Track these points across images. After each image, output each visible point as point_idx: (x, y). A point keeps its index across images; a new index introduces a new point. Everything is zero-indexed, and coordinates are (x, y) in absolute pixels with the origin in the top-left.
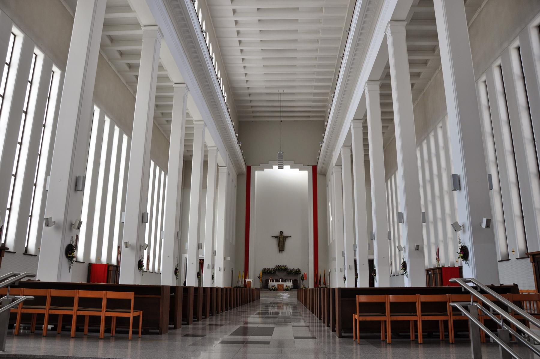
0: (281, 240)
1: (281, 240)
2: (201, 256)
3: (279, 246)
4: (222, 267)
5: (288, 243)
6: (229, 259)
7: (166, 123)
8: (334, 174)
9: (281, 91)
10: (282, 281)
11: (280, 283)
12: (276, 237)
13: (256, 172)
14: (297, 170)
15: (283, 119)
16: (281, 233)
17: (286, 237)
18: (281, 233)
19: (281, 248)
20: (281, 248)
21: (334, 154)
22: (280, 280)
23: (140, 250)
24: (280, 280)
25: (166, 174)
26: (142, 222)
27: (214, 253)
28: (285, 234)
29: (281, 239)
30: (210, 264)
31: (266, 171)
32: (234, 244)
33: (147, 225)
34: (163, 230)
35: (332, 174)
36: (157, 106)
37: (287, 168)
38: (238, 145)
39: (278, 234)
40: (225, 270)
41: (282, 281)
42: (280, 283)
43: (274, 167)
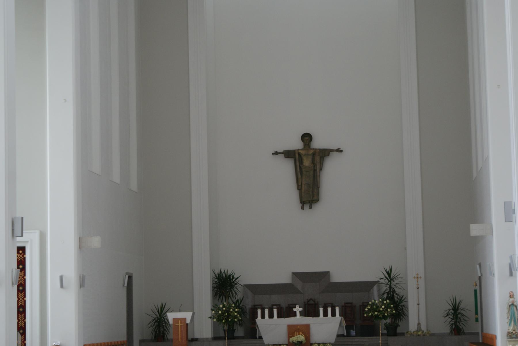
0: (308, 164)
1: (308, 164)
3: (299, 187)
4: (71, 274)
5: (332, 174)
10: (302, 314)
11: (298, 320)
12: (288, 154)
16: (307, 138)
17: (325, 153)
18: (307, 138)
19: (309, 193)
20: (309, 193)
22: (298, 309)
24: (298, 309)
28: (318, 144)
29: (307, 162)
32: (134, 185)
39: (297, 144)
41: (302, 314)
42: (298, 320)
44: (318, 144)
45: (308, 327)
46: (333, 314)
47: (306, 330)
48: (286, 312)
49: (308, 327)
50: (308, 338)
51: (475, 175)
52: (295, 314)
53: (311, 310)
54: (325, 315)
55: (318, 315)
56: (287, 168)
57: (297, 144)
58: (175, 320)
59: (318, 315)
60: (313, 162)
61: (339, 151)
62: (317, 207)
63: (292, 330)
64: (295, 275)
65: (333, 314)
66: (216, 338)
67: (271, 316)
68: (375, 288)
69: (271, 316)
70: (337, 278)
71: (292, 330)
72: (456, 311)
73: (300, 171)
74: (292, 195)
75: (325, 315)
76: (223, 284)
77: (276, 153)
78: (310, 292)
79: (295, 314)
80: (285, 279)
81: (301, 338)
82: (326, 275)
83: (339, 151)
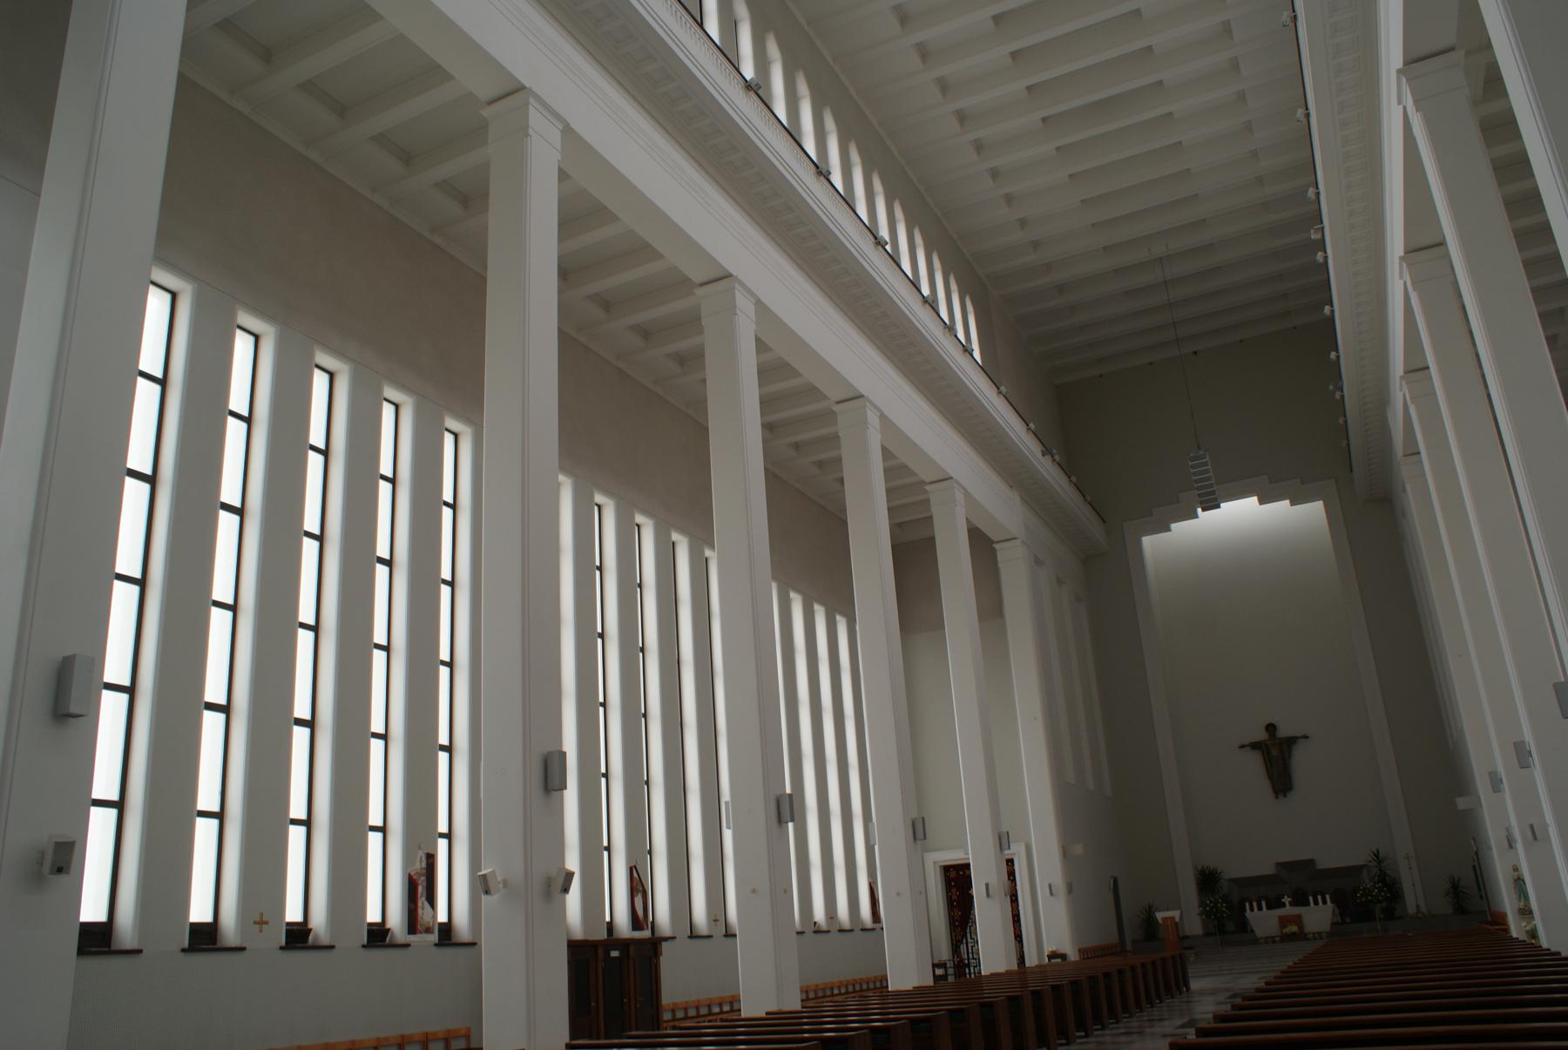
0: (1276, 754)
1: (1276, 754)
3: (1271, 777)
5: (1301, 760)
6: (1078, 849)
12: (1255, 746)
14: (1285, 504)
16: (1271, 728)
17: (1291, 741)
18: (1271, 728)
19: (1282, 783)
20: (1282, 783)
21: (1390, 415)
22: (1286, 900)
24: (1286, 900)
28: (1283, 732)
29: (1274, 752)
31: (1182, 530)
35: (1404, 490)
39: (1261, 735)
40: (1070, 889)
42: (1289, 910)
45: (1299, 916)
46: (1325, 902)
47: (1297, 919)
48: (1274, 903)
49: (1299, 916)
50: (1301, 927)
52: (1284, 905)
53: (1300, 900)
54: (1316, 903)
55: (1308, 904)
56: (1255, 761)
57: (1261, 735)
58: (1165, 919)
59: (1308, 904)
61: (1306, 737)
63: (1284, 922)
64: (1280, 865)
65: (1325, 902)
66: (1207, 934)
67: (1260, 908)
68: (1365, 872)
69: (1260, 908)
70: (1325, 862)
71: (1284, 922)
72: (1455, 889)
73: (1269, 763)
74: (1265, 786)
75: (1316, 903)
76: (1208, 880)
77: (1242, 747)
79: (1284, 905)
80: (1268, 869)
81: (1294, 928)
82: (1311, 862)
83: (1306, 737)
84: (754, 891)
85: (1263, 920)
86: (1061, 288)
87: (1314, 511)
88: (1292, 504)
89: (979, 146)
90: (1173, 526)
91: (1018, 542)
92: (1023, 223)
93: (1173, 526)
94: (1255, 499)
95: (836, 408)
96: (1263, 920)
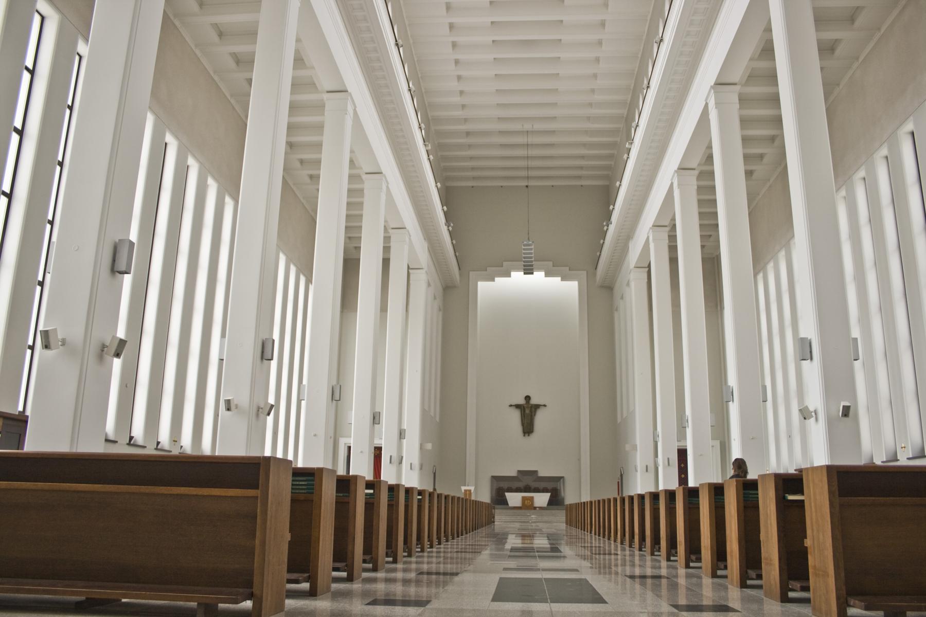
0: (528, 412)
1: (528, 412)
2: (377, 442)
3: (523, 424)
5: (540, 418)
6: (429, 446)
7: (308, 180)
8: (632, 284)
9: (528, 126)
12: (518, 406)
13: (479, 283)
14: (557, 280)
15: (532, 183)
16: (528, 398)
17: (537, 407)
18: (528, 398)
19: (528, 428)
20: (528, 428)
21: (631, 245)
23: (257, 415)
25: (309, 281)
26: (262, 358)
27: (401, 434)
28: (534, 401)
29: (527, 411)
30: (395, 455)
31: (500, 282)
32: (438, 419)
33: (274, 364)
34: (305, 382)
35: (628, 284)
36: (290, 145)
37: (539, 276)
38: (446, 228)
39: (522, 401)
43: (513, 273)
44: (534, 401)
47: (532, 498)
49: (532, 498)
51: (619, 420)
56: (516, 415)
57: (522, 401)
58: (466, 491)
60: (531, 411)
62: (534, 436)
64: (519, 471)
70: (542, 473)
71: (524, 499)
77: (511, 406)
78: (528, 482)
80: (513, 473)
82: (536, 472)
83: (545, 406)
84: (315, 435)
85: (515, 499)
86: (468, 134)
87: (572, 287)
88: (562, 280)
89: (454, 45)
90: (496, 279)
91: (423, 271)
92: (461, 92)
93: (496, 279)
94: (543, 273)
95: (364, 177)
96: (515, 499)
